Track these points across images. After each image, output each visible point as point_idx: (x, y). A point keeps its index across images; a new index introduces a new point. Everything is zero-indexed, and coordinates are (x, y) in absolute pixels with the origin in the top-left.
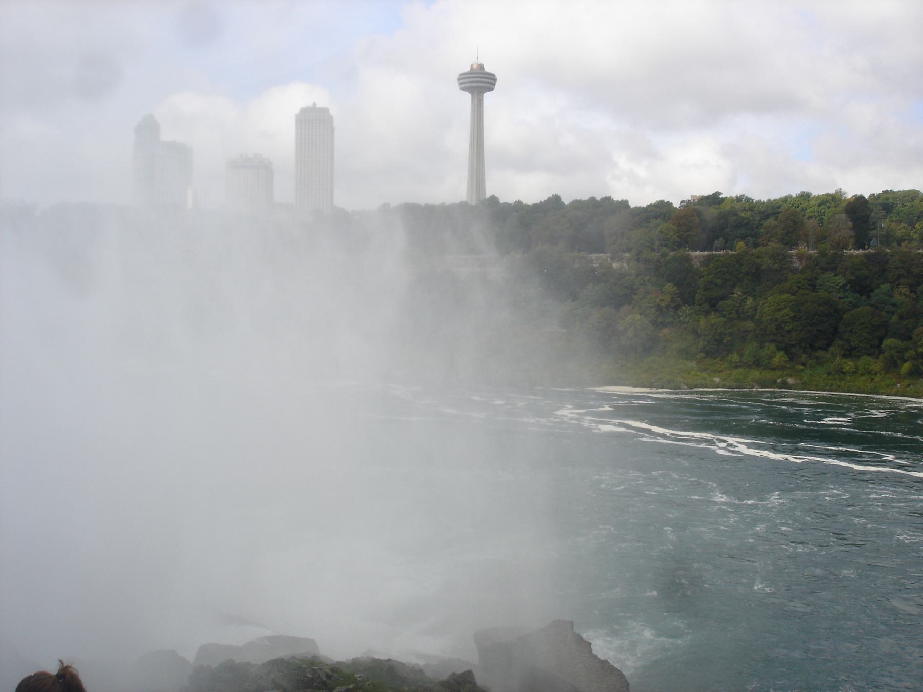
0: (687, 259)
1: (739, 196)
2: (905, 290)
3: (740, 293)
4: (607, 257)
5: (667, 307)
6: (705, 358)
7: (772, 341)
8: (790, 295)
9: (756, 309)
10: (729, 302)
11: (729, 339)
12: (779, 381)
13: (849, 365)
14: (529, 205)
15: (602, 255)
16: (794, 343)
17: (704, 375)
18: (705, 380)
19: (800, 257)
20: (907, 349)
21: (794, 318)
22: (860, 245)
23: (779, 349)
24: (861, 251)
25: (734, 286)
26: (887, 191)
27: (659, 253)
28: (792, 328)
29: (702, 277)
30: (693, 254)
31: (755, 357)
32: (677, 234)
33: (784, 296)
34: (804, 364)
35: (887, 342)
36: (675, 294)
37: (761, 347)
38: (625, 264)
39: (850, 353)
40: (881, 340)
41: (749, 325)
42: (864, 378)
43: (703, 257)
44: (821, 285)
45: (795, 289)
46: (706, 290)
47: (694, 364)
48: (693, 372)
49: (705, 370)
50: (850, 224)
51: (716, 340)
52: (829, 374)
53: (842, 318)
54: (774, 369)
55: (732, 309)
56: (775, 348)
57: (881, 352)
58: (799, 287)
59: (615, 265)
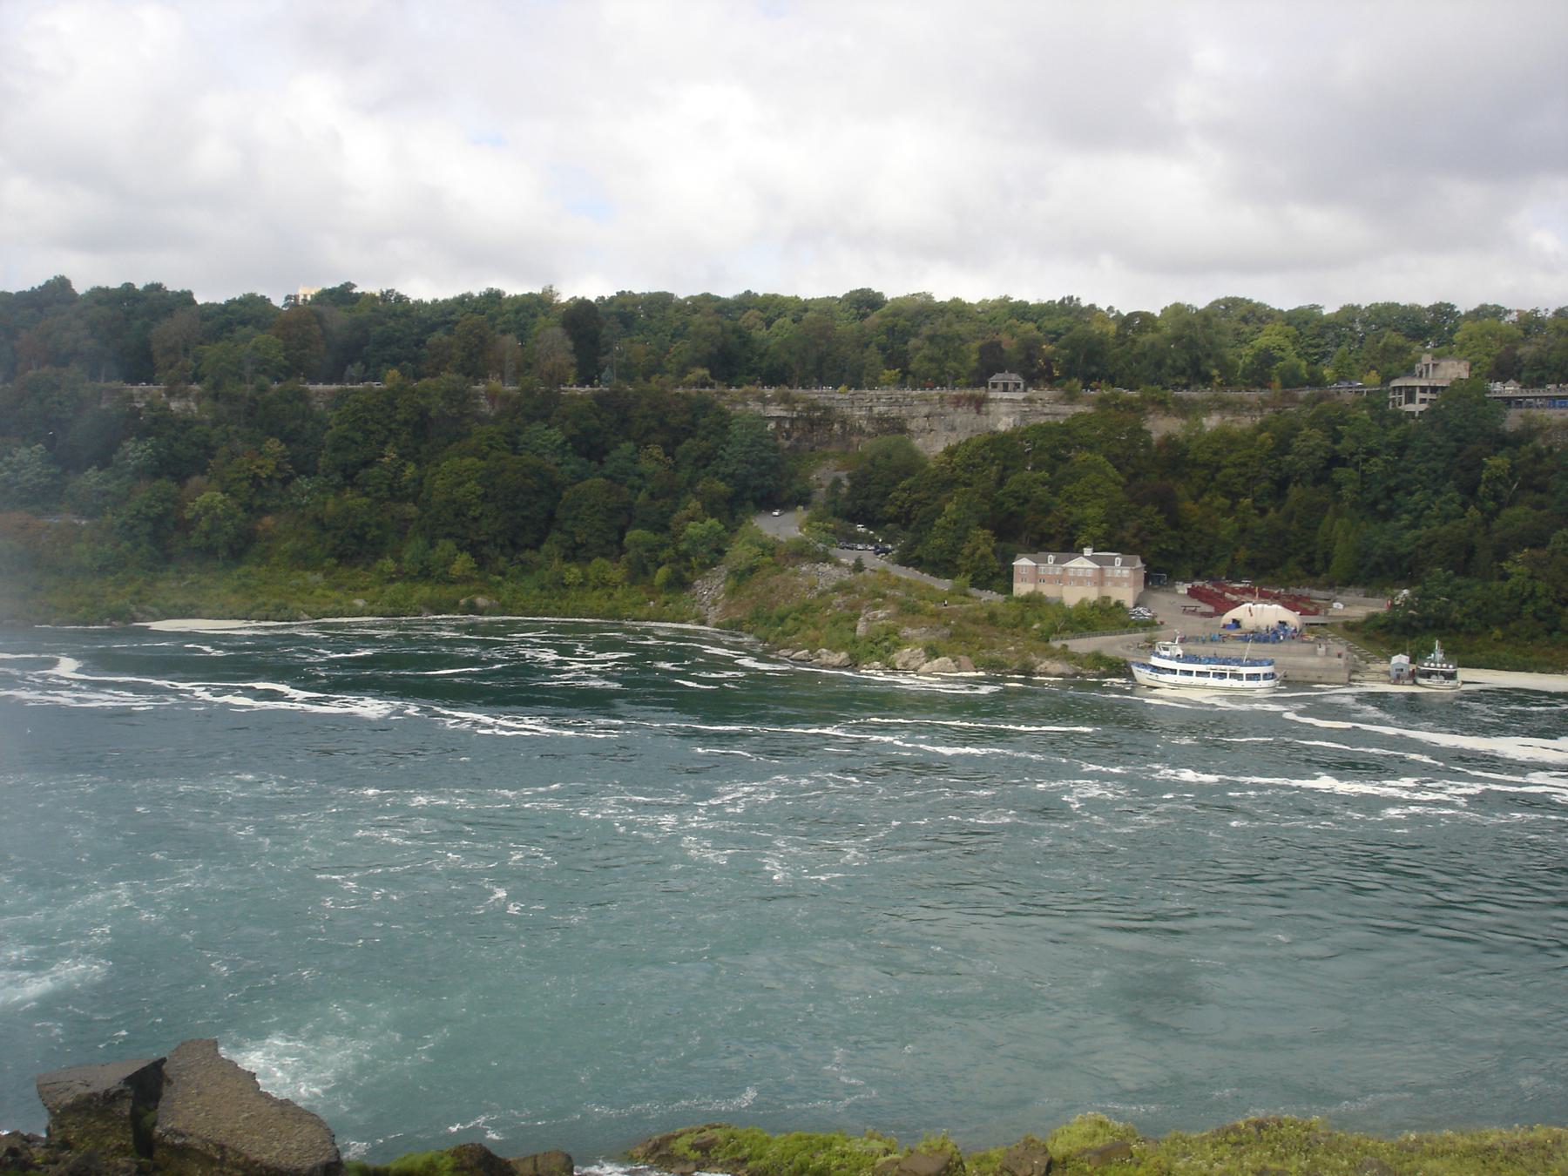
0: (303, 396)
1: (384, 290)
2: (657, 451)
3: (394, 456)
4: (160, 390)
5: (270, 479)
6: (337, 565)
7: (449, 535)
8: (476, 460)
9: (421, 484)
10: (375, 470)
11: (377, 532)
12: (463, 601)
13: (573, 573)
14: (11, 294)
15: (152, 386)
16: (483, 538)
17: (337, 595)
18: (339, 603)
19: (492, 396)
20: (662, 546)
21: (484, 498)
22: (585, 380)
23: (461, 550)
24: (588, 388)
25: (384, 443)
26: (623, 292)
27: (253, 386)
28: (481, 514)
29: (331, 428)
30: (312, 388)
31: (422, 563)
32: (283, 354)
33: (468, 461)
34: (502, 574)
35: (633, 535)
36: (284, 457)
37: (432, 546)
38: (192, 404)
39: (574, 553)
40: (622, 532)
41: (411, 509)
42: (596, 593)
43: (332, 393)
44: (526, 444)
45: (486, 449)
46: (336, 450)
47: (319, 577)
48: (318, 592)
49: (338, 587)
50: (570, 344)
51: (355, 536)
52: (542, 588)
53: (560, 498)
54: (453, 582)
55: (381, 483)
56: (455, 547)
57: (623, 550)
58: (491, 447)
59: (174, 405)
